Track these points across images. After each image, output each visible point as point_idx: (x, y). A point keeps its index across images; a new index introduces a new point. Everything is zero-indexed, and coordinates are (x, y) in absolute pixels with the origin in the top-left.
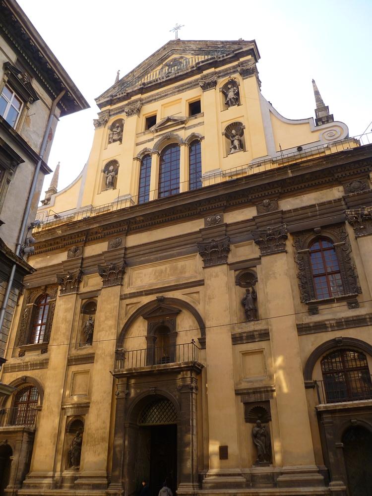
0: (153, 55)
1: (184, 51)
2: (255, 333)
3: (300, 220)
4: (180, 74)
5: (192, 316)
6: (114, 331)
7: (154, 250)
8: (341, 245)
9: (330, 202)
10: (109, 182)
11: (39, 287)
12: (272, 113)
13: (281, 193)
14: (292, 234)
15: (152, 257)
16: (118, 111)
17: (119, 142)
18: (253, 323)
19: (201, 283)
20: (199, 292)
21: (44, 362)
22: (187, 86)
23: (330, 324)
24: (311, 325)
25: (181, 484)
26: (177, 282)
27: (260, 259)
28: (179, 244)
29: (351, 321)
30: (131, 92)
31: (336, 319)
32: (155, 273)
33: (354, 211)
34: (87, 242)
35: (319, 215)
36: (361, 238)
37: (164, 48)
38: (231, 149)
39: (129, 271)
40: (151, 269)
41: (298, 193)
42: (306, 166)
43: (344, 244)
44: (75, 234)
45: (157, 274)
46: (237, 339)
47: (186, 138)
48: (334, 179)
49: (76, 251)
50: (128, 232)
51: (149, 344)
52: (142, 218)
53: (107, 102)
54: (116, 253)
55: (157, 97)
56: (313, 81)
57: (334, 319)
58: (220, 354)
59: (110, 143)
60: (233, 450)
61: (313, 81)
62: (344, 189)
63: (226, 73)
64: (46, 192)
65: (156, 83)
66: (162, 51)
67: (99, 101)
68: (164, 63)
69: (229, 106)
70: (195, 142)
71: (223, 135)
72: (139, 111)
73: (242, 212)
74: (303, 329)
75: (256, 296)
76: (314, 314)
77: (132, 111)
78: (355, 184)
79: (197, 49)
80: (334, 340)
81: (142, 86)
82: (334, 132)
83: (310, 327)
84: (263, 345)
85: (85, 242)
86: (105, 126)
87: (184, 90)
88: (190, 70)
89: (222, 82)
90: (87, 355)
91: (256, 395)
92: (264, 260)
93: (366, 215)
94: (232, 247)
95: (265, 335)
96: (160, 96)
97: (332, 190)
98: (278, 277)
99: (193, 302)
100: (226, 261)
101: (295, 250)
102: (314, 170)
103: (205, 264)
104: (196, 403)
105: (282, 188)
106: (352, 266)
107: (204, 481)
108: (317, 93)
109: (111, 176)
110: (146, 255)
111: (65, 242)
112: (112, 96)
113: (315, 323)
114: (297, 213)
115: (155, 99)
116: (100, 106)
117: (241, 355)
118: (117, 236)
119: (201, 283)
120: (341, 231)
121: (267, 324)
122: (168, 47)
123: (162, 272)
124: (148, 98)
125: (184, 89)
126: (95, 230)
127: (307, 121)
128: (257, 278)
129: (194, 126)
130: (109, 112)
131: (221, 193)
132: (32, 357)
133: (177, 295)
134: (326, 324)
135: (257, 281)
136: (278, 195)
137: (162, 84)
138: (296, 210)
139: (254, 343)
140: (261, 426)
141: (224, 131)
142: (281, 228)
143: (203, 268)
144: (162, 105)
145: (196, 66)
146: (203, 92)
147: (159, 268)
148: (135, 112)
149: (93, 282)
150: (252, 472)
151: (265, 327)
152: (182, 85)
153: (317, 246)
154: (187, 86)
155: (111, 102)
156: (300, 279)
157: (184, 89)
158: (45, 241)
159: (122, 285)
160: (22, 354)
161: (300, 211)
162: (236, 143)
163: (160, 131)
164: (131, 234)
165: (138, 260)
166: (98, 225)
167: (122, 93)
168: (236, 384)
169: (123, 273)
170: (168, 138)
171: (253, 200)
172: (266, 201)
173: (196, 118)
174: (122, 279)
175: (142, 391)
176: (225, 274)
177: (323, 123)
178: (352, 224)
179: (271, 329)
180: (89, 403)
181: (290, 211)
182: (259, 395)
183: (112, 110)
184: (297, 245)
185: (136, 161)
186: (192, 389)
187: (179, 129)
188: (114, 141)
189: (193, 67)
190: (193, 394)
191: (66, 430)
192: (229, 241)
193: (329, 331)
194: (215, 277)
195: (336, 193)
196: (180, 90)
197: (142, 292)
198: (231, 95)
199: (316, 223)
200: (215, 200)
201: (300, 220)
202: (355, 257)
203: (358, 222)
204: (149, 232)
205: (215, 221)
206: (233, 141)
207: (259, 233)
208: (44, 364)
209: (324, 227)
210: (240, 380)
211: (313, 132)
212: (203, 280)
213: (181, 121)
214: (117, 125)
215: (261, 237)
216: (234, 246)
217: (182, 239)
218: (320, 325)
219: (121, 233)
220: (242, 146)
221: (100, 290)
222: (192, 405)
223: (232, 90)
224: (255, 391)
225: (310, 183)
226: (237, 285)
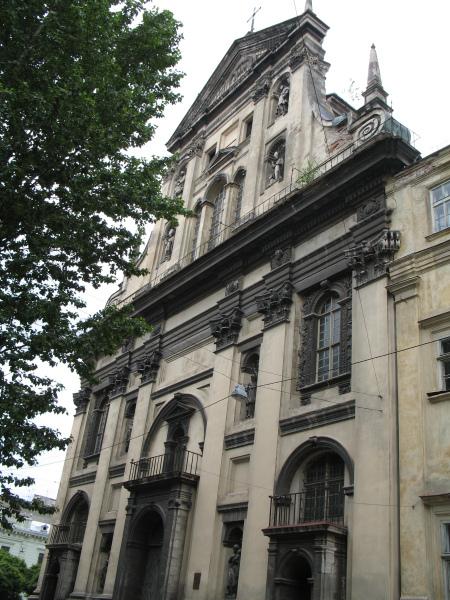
19: (209, 374)
23: (311, 419)
24: (293, 421)
28: (201, 325)
35: (328, 261)
37: (229, 53)
39: (163, 363)
46: (231, 442)
56: (373, 47)
60: (204, 579)
61: (373, 47)
72: (200, 148)
74: (287, 427)
78: (370, 206)
80: (307, 442)
92: (267, 336)
93: (367, 253)
94: (245, 321)
100: (236, 340)
108: (374, 65)
119: (209, 374)
132: (90, 468)
138: (305, 259)
149: (135, 381)
152: (239, 102)
159: (154, 382)
160: (85, 467)
162: (277, 168)
169: (156, 367)
174: (156, 374)
181: (299, 262)
208: (92, 477)
209: (333, 279)
212: (212, 370)
221: (137, 390)
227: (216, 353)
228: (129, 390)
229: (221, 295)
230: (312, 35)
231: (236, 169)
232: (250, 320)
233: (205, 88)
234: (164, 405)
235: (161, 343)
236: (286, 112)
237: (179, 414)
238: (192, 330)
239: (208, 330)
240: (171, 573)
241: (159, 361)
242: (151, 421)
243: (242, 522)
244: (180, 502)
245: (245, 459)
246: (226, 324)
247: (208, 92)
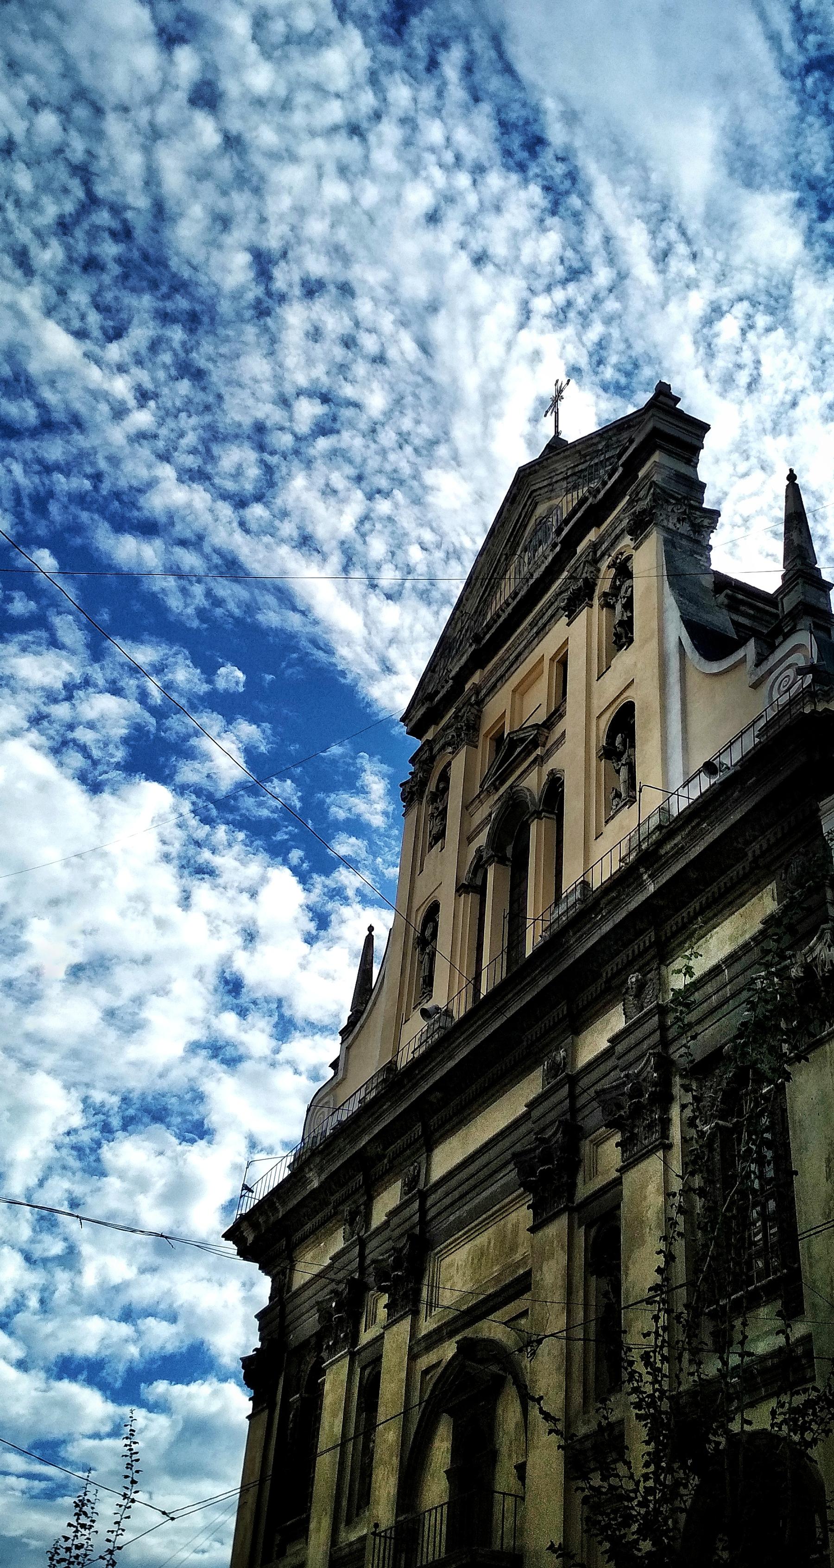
6: (395, 1461)
7: (465, 1187)
35: (733, 996)
45: (476, 1261)
50: (430, 1143)
66: (509, 510)
122: (519, 490)
131: (544, 982)
136: (652, 952)
211: (755, 686)
215: (620, 1107)
228: (365, 1337)
229: (531, 1086)
230: (669, 453)
231: (545, 778)
234: (440, 1370)
235: (423, 1211)
236: (631, 641)
238: (481, 1175)
239: (510, 1175)
242: (416, 1415)
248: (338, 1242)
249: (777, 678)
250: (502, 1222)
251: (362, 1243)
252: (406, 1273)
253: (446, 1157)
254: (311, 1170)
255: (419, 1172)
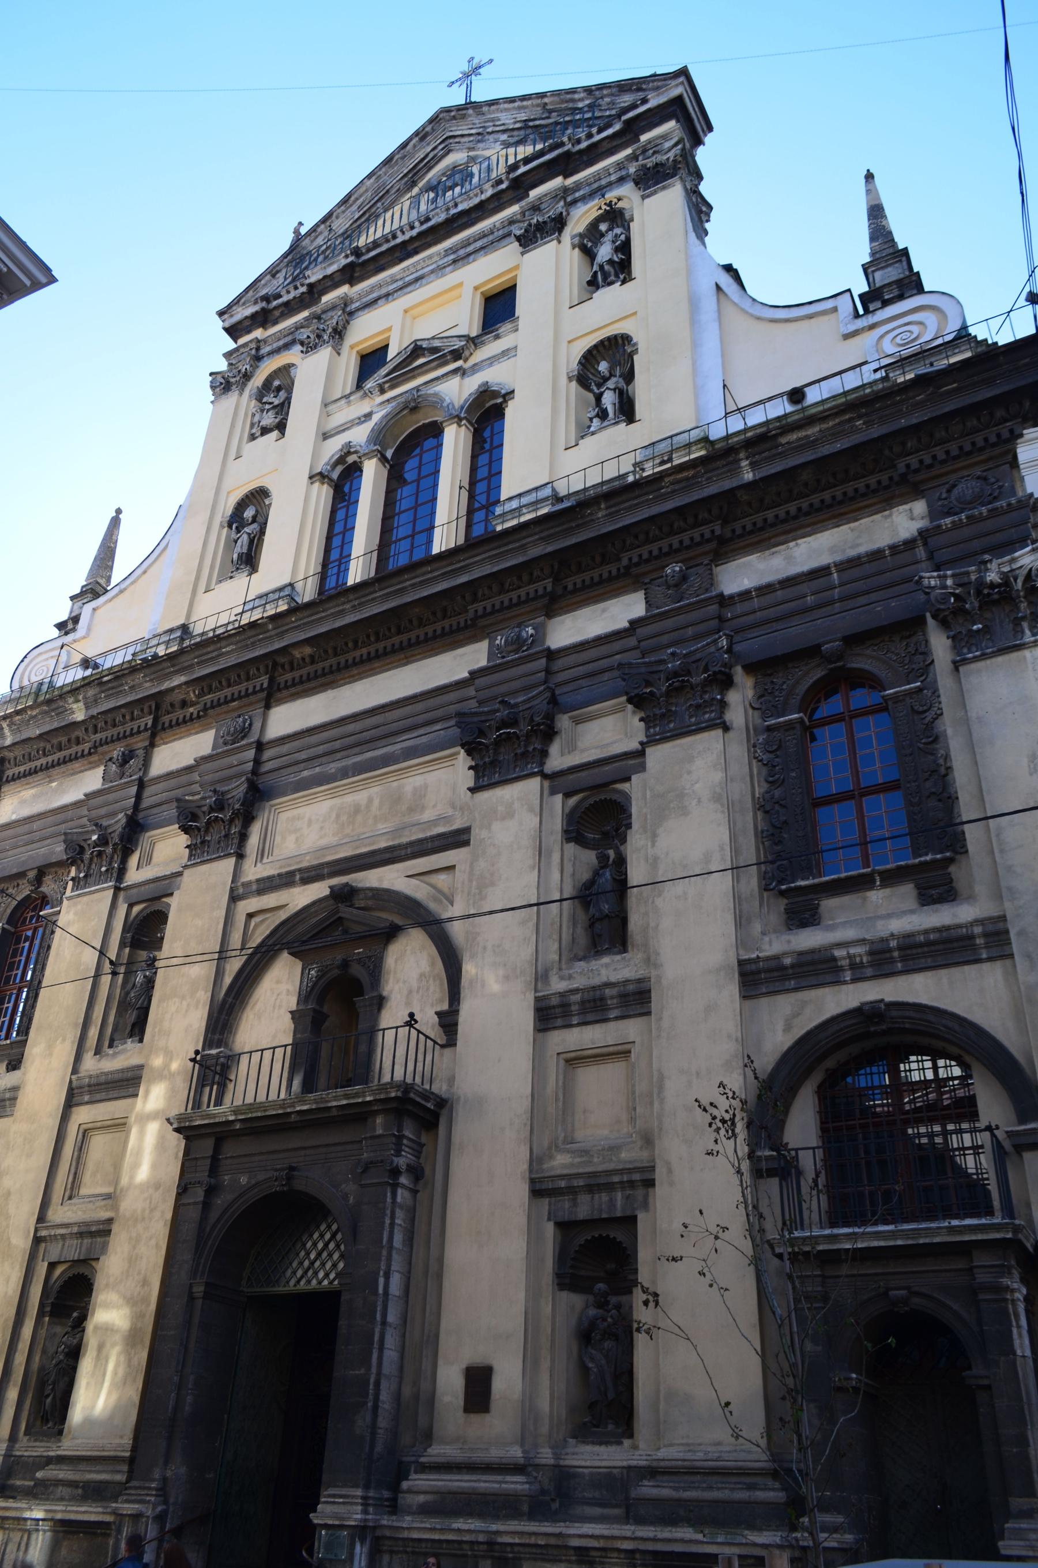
0: (388, 161)
1: (481, 136)
2: (608, 992)
3: (777, 620)
4: (460, 208)
5: (429, 943)
6: (204, 997)
7: (337, 745)
8: (910, 693)
9: (876, 555)
10: (240, 556)
11: (22, 875)
12: (726, 295)
13: (722, 541)
14: (750, 669)
15: (333, 767)
16: (281, 343)
17: (275, 434)
18: (606, 960)
19: (459, 839)
20: (453, 867)
21: (7, 1095)
22: (479, 244)
23: (850, 957)
24: (787, 961)
25: (331, 1491)
26: (393, 839)
27: (640, 754)
29: (921, 945)
30: (319, 281)
31: (872, 942)
32: (338, 816)
33: (953, 576)
34: (156, 734)
35: (842, 599)
36: (973, 666)
38: (591, 419)
40: (328, 804)
41: (776, 536)
42: (799, 439)
43: (920, 690)
44: (123, 710)
45: (344, 818)
47: (462, 402)
48: (896, 478)
49: (125, 759)
51: (299, 1036)
52: (308, 650)
53: (253, 316)
54: (234, 760)
55: (391, 287)
57: (862, 941)
58: (496, 1062)
59: (253, 437)
60: (507, 1381)
62: (929, 506)
63: (595, 186)
64: (72, 598)
65: (393, 243)
67: (232, 316)
68: (421, 184)
69: (598, 288)
70: (487, 413)
71: (570, 379)
73: (604, 611)
75: (626, 874)
76: (804, 924)
77: (319, 337)
79: (518, 125)
81: (351, 259)
82: (915, 329)
83: (783, 968)
84: (630, 1029)
85: (153, 735)
86: (241, 394)
87: (472, 257)
88: (489, 192)
89: (581, 217)
90: (122, 1071)
91: (597, 1196)
92: (655, 755)
94: (563, 722)
95: (636, 999)
96: (400, 283)
97: (890, 515)
98: (694, 809)
99: (436, 900)
100: (542, 764)
101: (760, 721)
102: (826, 450)
103: (477, 778)
104: (412, 1220)
105: (725, 522)
106: (941, 761)
107: (405, 1485)
109: (245, 537)
110: (316, 762)
111: (98, 736)
112: (266, 298)
113: (801, 954)
114: (769, 599)
115: (387, 295)
116: (233, 331)
117: (562, 1063)
118: (240, 708)
119: (459, 839)
120: (912, 649)
121: (648, 961)
123: (357, 810)
124: (369, 293)
125: (469, 255)
126: (177, 697)
127: (829, 305)
128: (631, 815)
129: (492, 360)
130: (258, 349)
131: (535, 552)
133: (391, 878)
134: (834, 959)
135: (629, 826)
136: (713, 545)
137: (410, 248)
139: (604, 1025)
140: (607, 1303)
141: (574, 365)
142: (712, 649)
143: (470, 789)
144: (406, 311)
145: (507, 178)
146: (523, 254)
147: (349, 799)
148: (326, 337)
150: (562, 1463)
151: (641, 973)
152: (466, 243)
153: (834, 705)
154: (479, 244)
155: (263, 319)
156: (766, 812)
157: (469, 255)
158: (41, 735)
159: (240, 856)
161: (779, 593)
162: (609, 400)
163: (393, 387)
164: (281, 701)
165: (293, 778)
166: (183, 679)
167: (296, 288)
168: (535, 1161)
170: (413, 405)
171: (634, 571)
172: (674, 568)
173: (497, 337)
175: (253, 1182)
176: (531, 810)
177: (886, 303)
178: (944, 624)
179: (659, 978)
180: (110, 1221)
181: (745, 595)
182: (605, 1197)
183: (265, 341)
184: (766, 703)
185: (317, 485)
186: (395, 1172)
187: (443, 376)
188: (265, 431)
189: (500, 182)
190: (400, 1191)
191: (42, 1305)
192: (553, 701)
193: (845, 983)
194: (503, 819)
195: (904, 521)
196: (460, 258)
197: (291, 874)
198: (605, 252)
199: (828, 628)
200: (520, 578)
201: (777, 620)
202: (950, 732)
203: (966, 612)
204: (330, 694)
205: (518, 643)
206: (602, 394)
207: (643, 670)
209: (855, 640)
210: (550, 1148)
211: (847, 336)
212: (467, 830)
213: (452, 352)
214: (276, 383)
215: (648, 684)
216: (570, 718)
217: (420, 707)
218: (813, 963)
219: (252, 698)
220: (627, 411)
222: (392, 1224)
223: (610, 236)
224: (592, 1181)
225: (815, 499)
226: (568, 840)
227: (473, 790)
232: (578, 721)
233: (345, 201)
234: (283, 915)
237: (341, 943)
240: (386, 1370)
241: (252, 804)
243: (630, 1221)
244: (402, 1162)
245: (621, 1053)
246: (513, 722)
247: (353, 212)
248: (92, 780)
249: (894, 329)
250: (395, 784)
251: (141, 785)
252: (222, 819)
253: (287, 718)
254: (77, 701)
255: (250, 725)
